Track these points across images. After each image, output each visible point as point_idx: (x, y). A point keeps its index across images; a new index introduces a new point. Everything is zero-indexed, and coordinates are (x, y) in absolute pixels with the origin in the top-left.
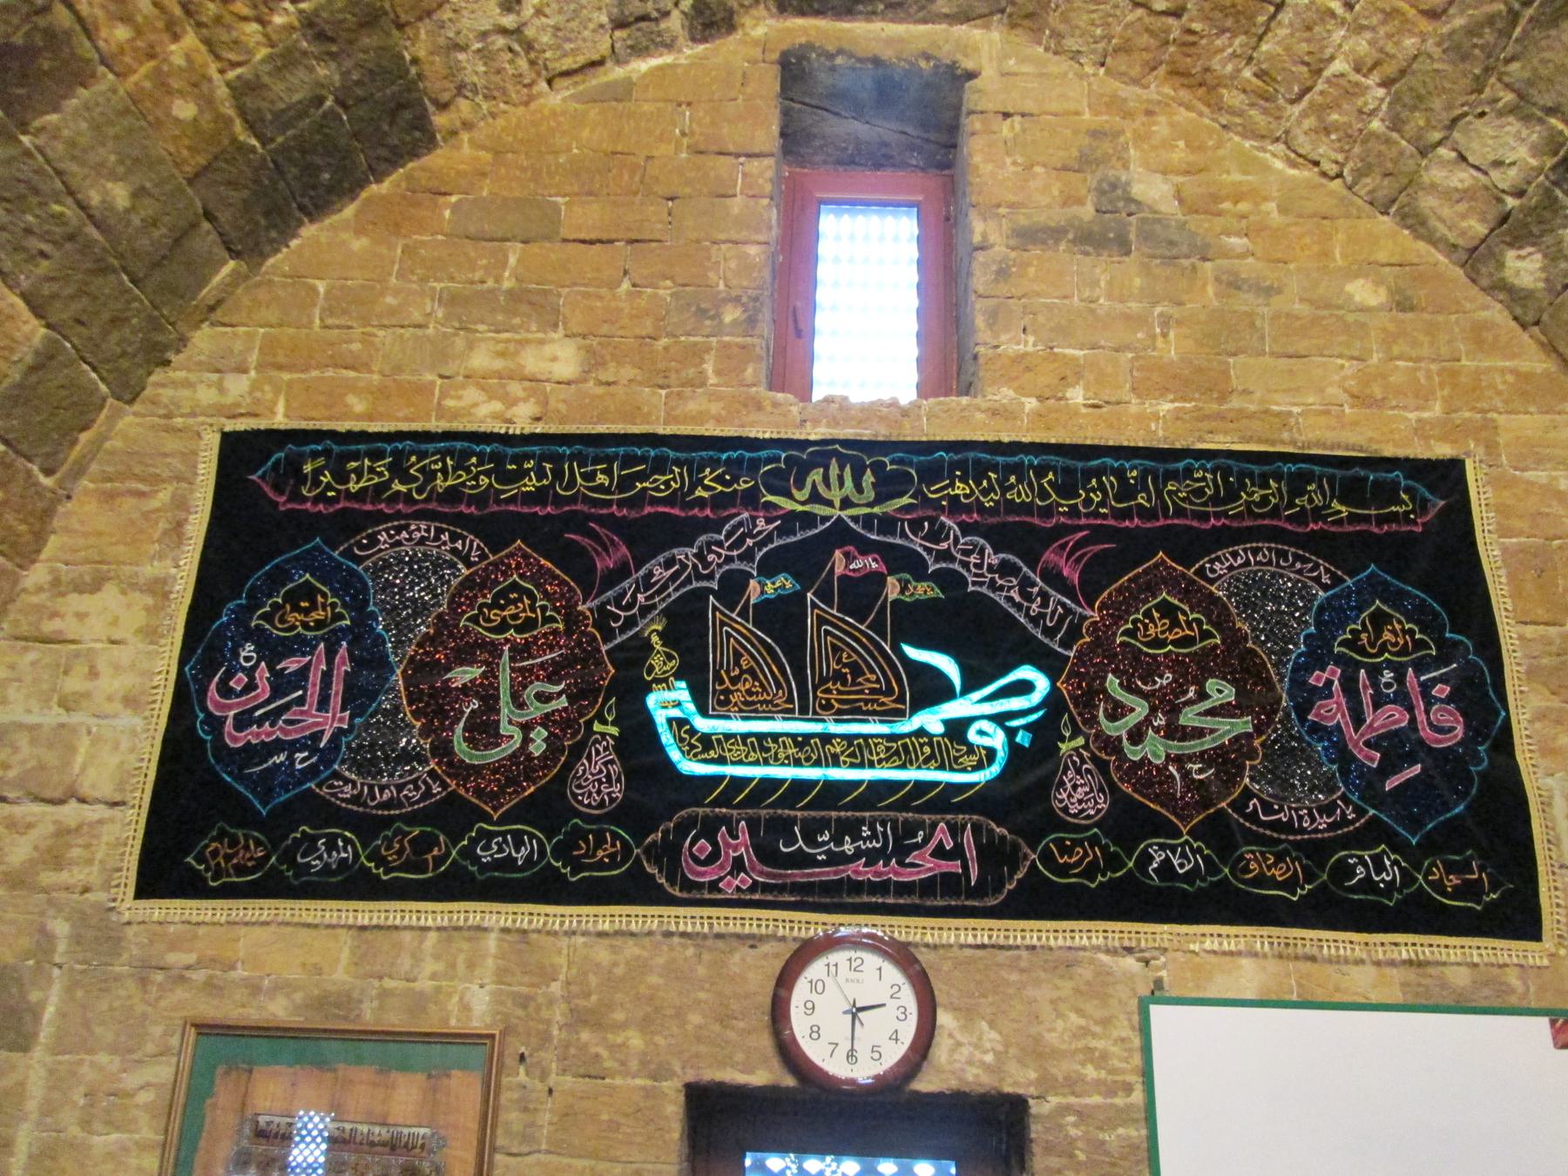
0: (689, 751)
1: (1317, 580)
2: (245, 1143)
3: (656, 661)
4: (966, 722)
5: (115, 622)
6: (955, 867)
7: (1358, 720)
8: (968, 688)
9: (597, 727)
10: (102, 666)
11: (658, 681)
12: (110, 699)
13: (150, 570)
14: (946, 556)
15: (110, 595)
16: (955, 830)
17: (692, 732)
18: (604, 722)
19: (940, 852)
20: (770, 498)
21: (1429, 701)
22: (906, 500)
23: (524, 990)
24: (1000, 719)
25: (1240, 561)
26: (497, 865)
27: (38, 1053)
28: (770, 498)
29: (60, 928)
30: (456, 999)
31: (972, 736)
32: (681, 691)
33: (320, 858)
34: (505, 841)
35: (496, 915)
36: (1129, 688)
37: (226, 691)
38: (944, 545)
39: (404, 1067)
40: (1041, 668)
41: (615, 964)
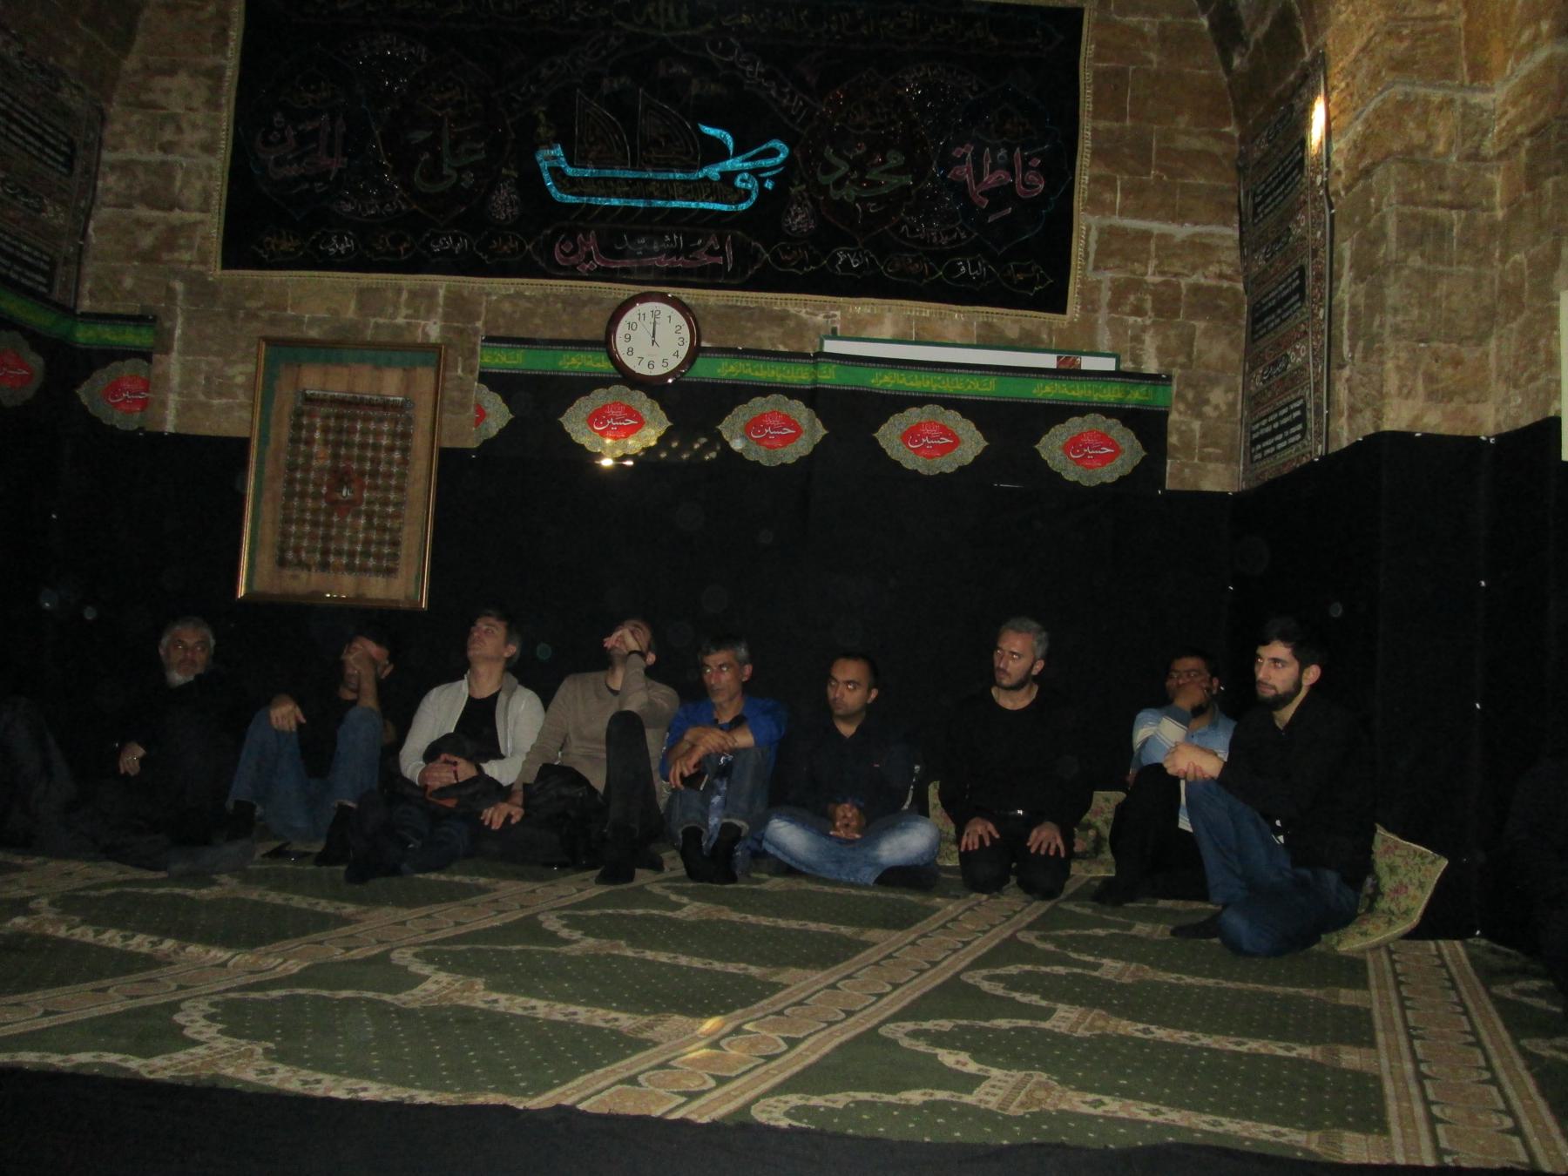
0: (561, 189)
1: (970, 88)
2: (299, 404)
3: (541, 130)
4: (735, 174)
5: (189, 95)
6: (720, 260)
7: (978, 177)
8: (736, 154)
9: (504, 171)
10: (184, 125)
11: (542, 143)
12: (192, 146)
13: (208, 62)
14: (732, 65)
15: (182, 79)
16: (722, 241)
17: (564, 175)
18: (508, 168)
19: (711, 252)
20: (621, 23)
21: (1026, 168)
22: (709, 26)
23: (460, 325)
24: (755, 172)
25: (921, 74)
26: (443, 253)
27: (174, 355)
28: (621, 23)
29: (179, 286)
30: (420, 330)
31: (738, 183)
32: (558, 151)
33: (334, 247)
34: (448, 240)
35: (442, 284)
36: (838, 153)
37: (267, 143)
38: (731, 58)
39: (389, 364)
40: (782, 139)
41: (514, 312)
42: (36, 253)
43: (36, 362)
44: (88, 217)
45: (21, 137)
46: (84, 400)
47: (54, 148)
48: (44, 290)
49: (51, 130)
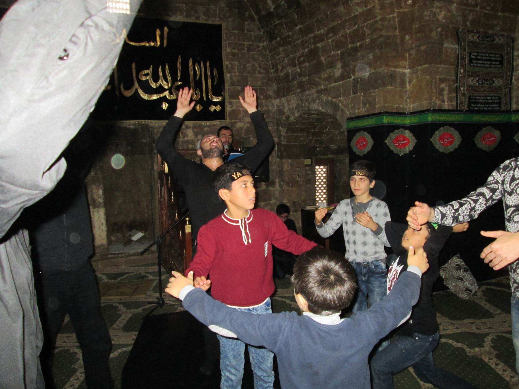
42: (493, 98)
43: (497, 134)
44: (512, 76)
45: (482, 63)
46: (517, 141)
47: (494, 61)
48: (498, 108)
49: (492, 55)
